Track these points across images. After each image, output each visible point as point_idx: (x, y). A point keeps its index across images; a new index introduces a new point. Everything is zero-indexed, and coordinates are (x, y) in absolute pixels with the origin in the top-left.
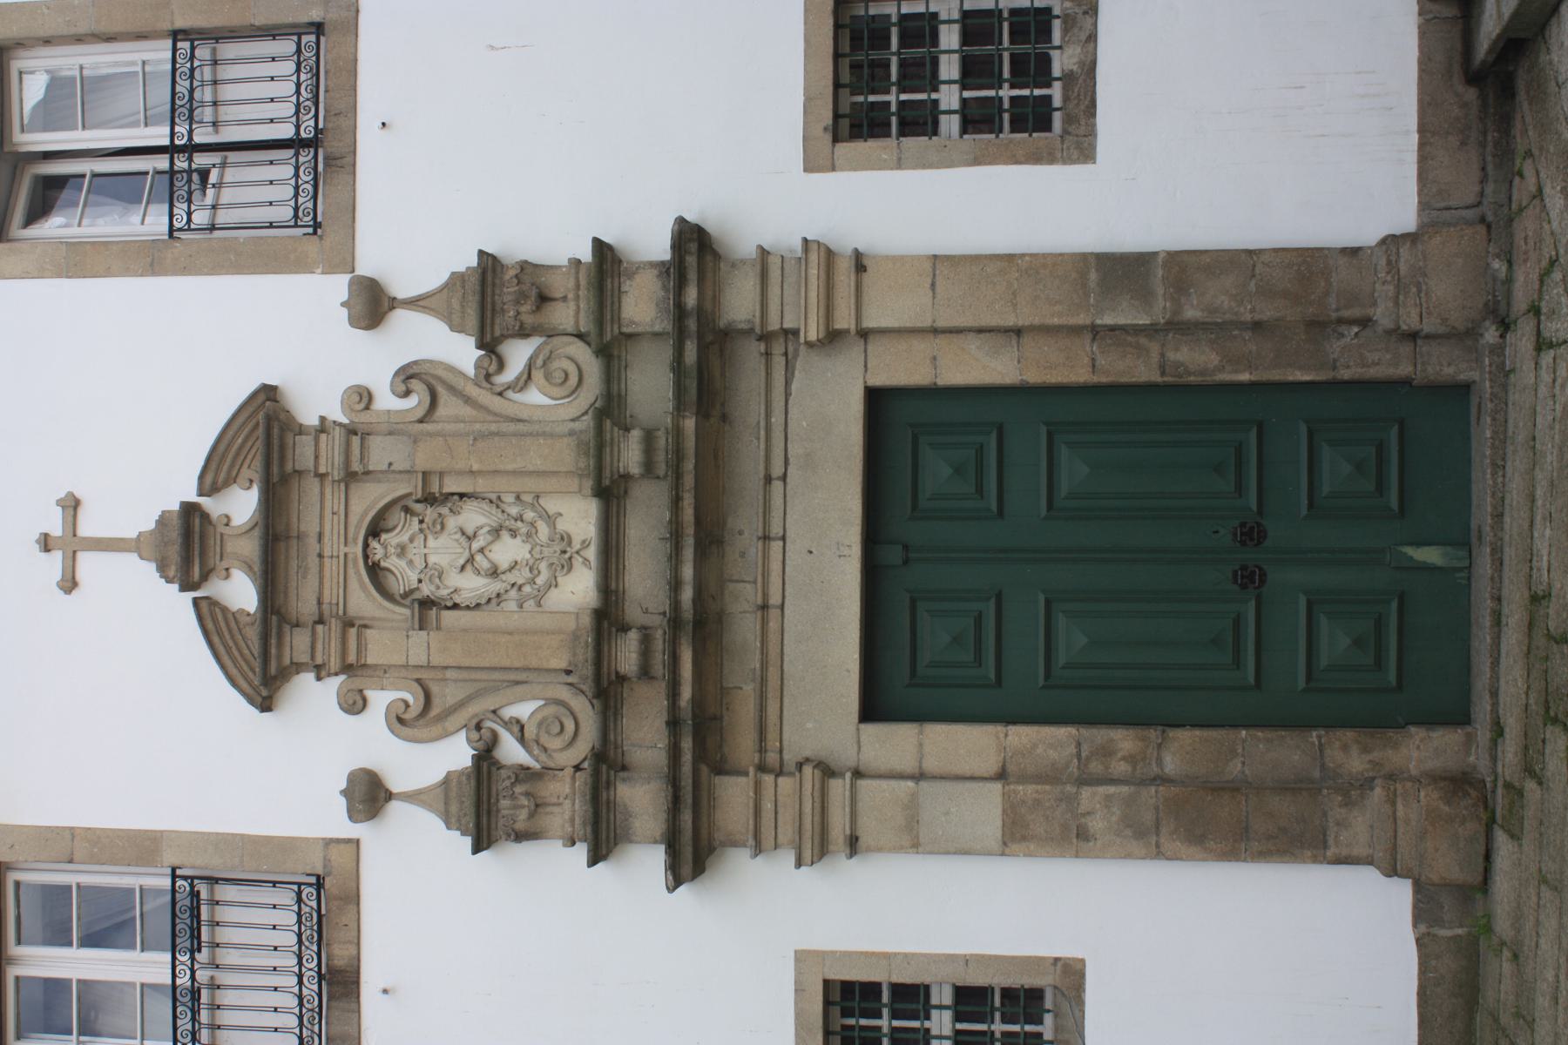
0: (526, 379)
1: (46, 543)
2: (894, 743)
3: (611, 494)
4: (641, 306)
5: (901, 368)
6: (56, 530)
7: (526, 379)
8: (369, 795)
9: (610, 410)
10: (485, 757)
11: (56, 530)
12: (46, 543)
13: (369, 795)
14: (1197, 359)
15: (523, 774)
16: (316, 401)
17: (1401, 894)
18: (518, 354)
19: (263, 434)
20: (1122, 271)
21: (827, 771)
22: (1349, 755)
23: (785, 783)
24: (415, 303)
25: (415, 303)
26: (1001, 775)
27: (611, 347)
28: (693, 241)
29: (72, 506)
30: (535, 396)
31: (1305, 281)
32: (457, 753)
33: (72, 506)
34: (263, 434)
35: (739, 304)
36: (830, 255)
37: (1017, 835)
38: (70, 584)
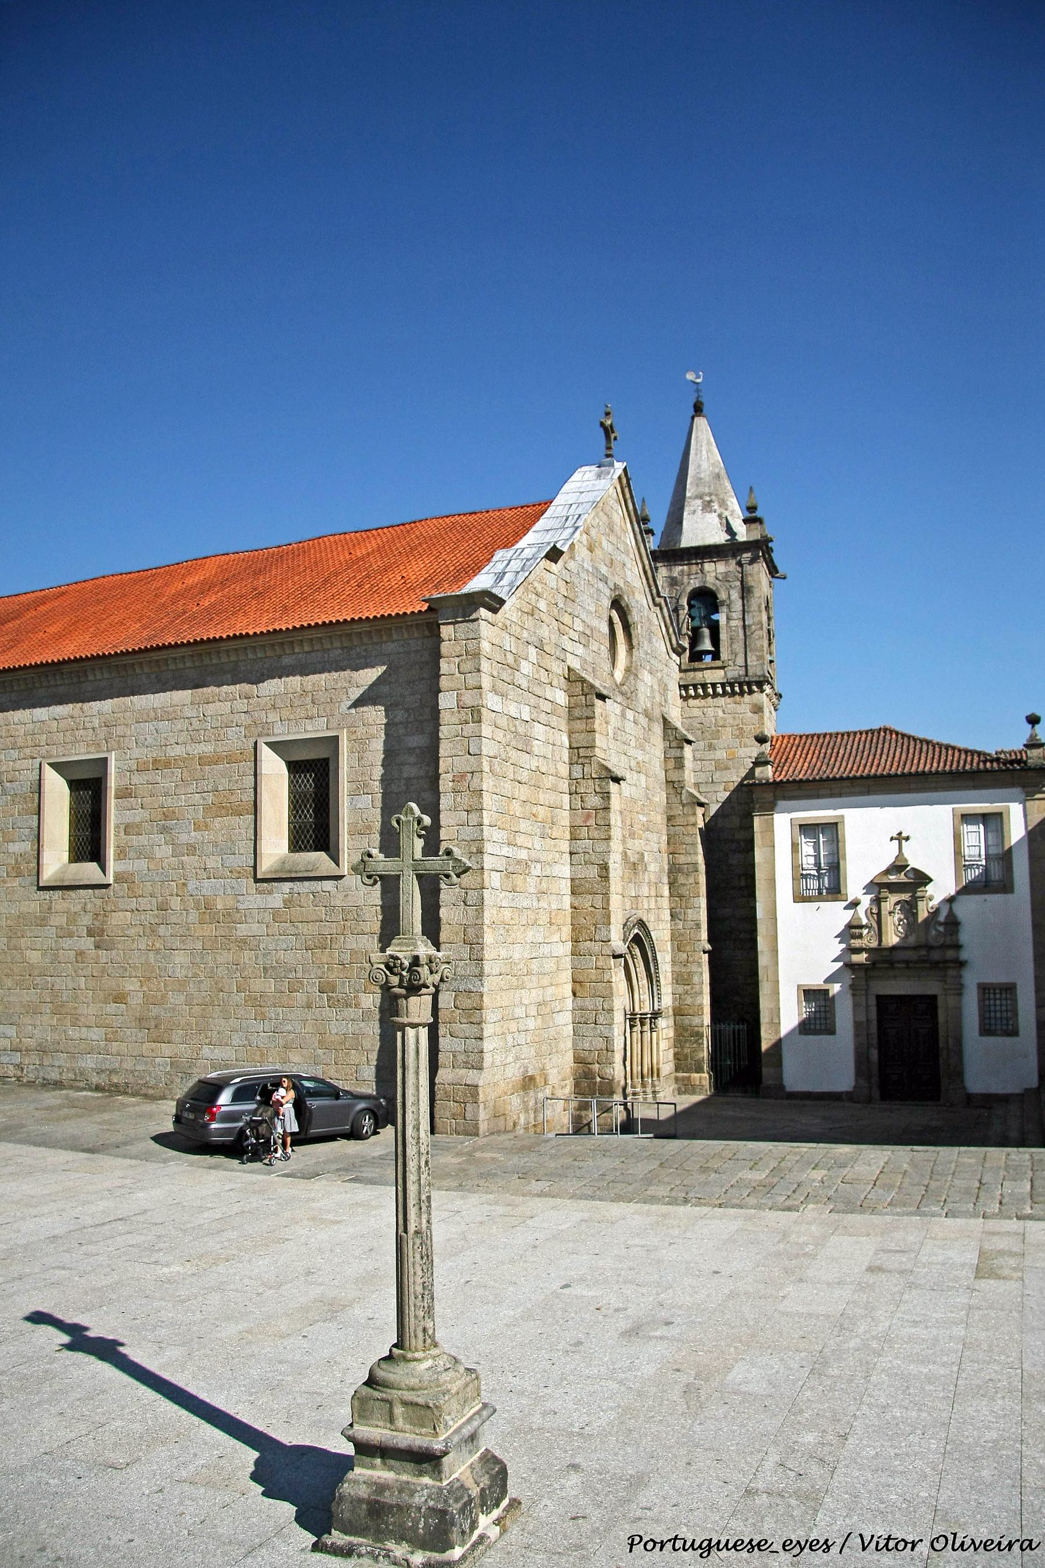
0: (936, 929)
1: (900, 834)
2: (873, 1001)
3: (915, 948)
4: (950, 954)
5: (940, 1001)
6: (904, 835)
7: (936, 929)
8: (855, 904)
9: (930, 948)
10: (866, 926)
11: (904, 835)
12: (900, 834)
13: (855, 904)
14: (944, 1054)
15: (861, 934)
16: (930, 888)
17: (850, 1089)
18: (941, 929)
19: (922, 879)
20: (959, 1040)
21: (866, 990)
22: (875, 1080)
23: (864, 983)
24: (951, 909)
25: (951, 909)
26: (868, 1020)
27: (943, 947)
28: (961, 964)
29: (907, 839)
30: (934, 932)
31: (959, 1074)
32: (865, 921)
33: (907, 839)
34: (922, 879)
35: (950, 972)
36: (960, 989)
37: (857, 1025)
38: (892, 839)
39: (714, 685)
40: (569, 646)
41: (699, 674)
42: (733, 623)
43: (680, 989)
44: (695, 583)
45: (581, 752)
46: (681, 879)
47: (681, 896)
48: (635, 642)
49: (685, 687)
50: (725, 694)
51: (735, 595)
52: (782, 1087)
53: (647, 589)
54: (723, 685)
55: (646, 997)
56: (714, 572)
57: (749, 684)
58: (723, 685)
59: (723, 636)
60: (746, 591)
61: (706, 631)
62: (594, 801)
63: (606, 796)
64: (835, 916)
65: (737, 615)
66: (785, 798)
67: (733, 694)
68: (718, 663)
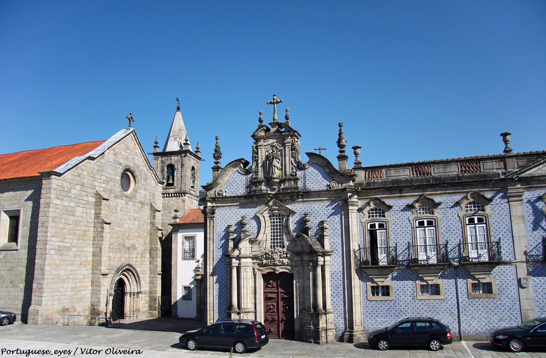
8: (198, 261)
13: (198, 261)
32: (201, 266)
37: (197, 297)
39: (171, 194)
40: (96, 183)
41: (168, 190)
42: (178, 175)
43: (151, 285)
44: (168, 163)
45: (97, 215)
46: (153, 252)
47: (152, 257)
48: (137, 181)
49: (164, 194)
50: (175, 196)
51: (179, 166)
52: (177, 316)
53: (147, 165)
54: (174, 194)
55: (136, 287)
56: (174, 159)
57: (181, 194)
58: (174, 194)
59: (175, 179)
60: (182, 165)
61: (171, 177)
62: (100, 229)
63: (103, 228)
64: (193, 264)
65: (179, 172)
66: (181, 229)
67: (177, 196)
68: (173, 187)
